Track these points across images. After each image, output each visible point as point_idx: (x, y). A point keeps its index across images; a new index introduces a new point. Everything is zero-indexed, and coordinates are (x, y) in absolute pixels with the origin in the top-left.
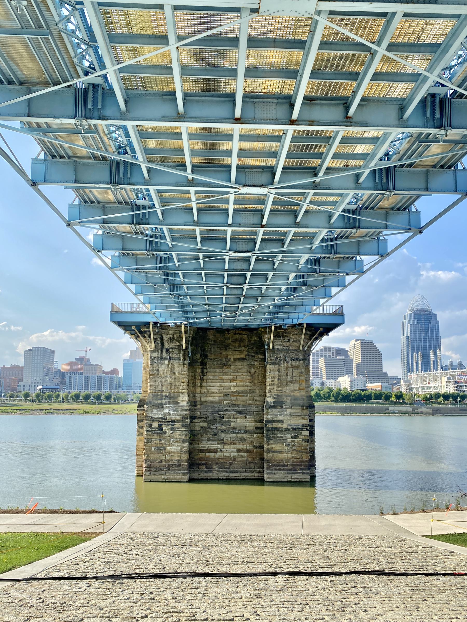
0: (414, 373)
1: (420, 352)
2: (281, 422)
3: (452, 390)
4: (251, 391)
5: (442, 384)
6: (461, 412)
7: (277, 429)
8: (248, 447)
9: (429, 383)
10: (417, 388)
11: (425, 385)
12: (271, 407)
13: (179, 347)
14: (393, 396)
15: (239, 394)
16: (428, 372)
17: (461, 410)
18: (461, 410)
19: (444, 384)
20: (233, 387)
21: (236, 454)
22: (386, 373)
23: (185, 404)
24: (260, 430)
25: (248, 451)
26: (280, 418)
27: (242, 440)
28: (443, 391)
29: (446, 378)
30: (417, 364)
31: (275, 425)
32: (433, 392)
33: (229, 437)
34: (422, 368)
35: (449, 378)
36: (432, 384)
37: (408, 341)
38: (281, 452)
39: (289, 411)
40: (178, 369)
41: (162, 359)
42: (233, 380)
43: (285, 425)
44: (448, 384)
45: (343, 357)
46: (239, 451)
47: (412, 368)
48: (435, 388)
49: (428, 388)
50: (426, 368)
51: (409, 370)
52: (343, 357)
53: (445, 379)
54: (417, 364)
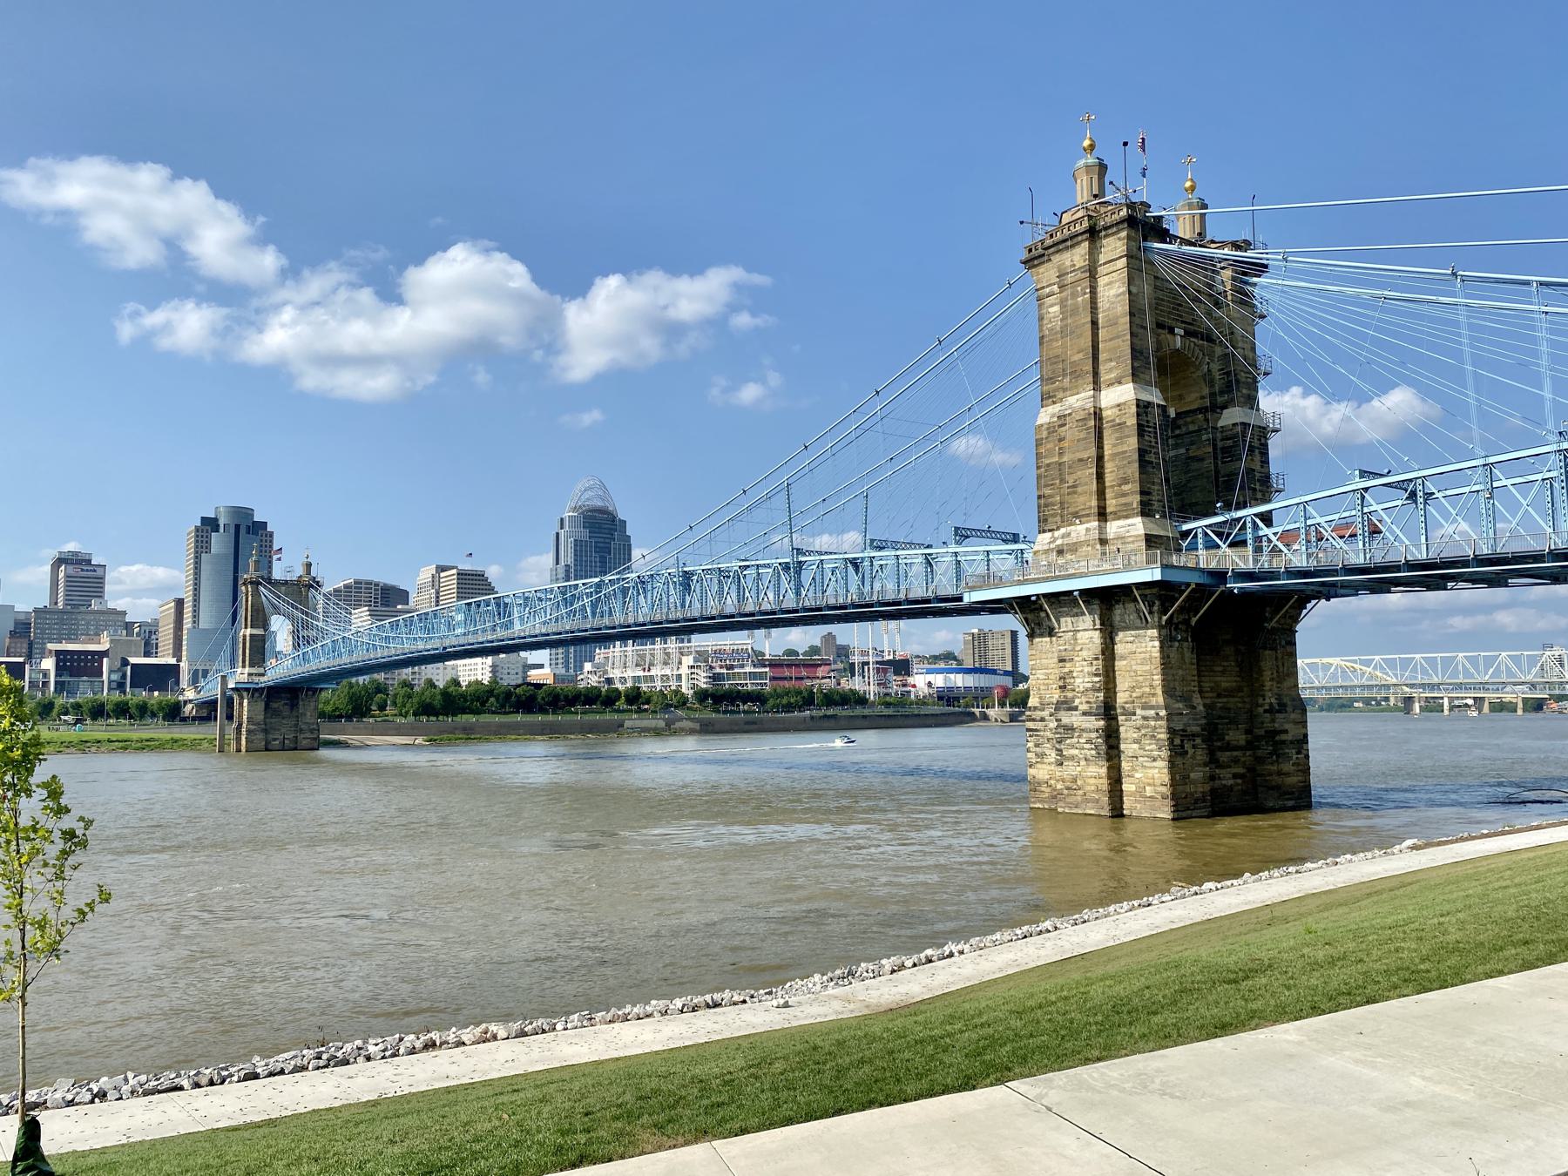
2: (1286, 732)
4: (1240, 689)
7: (1283, 742)
8: (1241, 770)
12: (1279, 712)
13: (1187, 622)
15: (1230, 693)
20: (1226, 682)
21: (1231, 782)
23: (1201, 708)
24: (1250, 745)
25: (1241, 776)
26: (1287, 726)
27: (1236, 761)
31: (1284, 737)
33: (1224, 757)
38: (1288, 774)
39: (1293, 716)
40: (1188, 655)
41: (1172, 639)
42: (1223, 673)
43: (1288, 737)
46: (1235, 776)
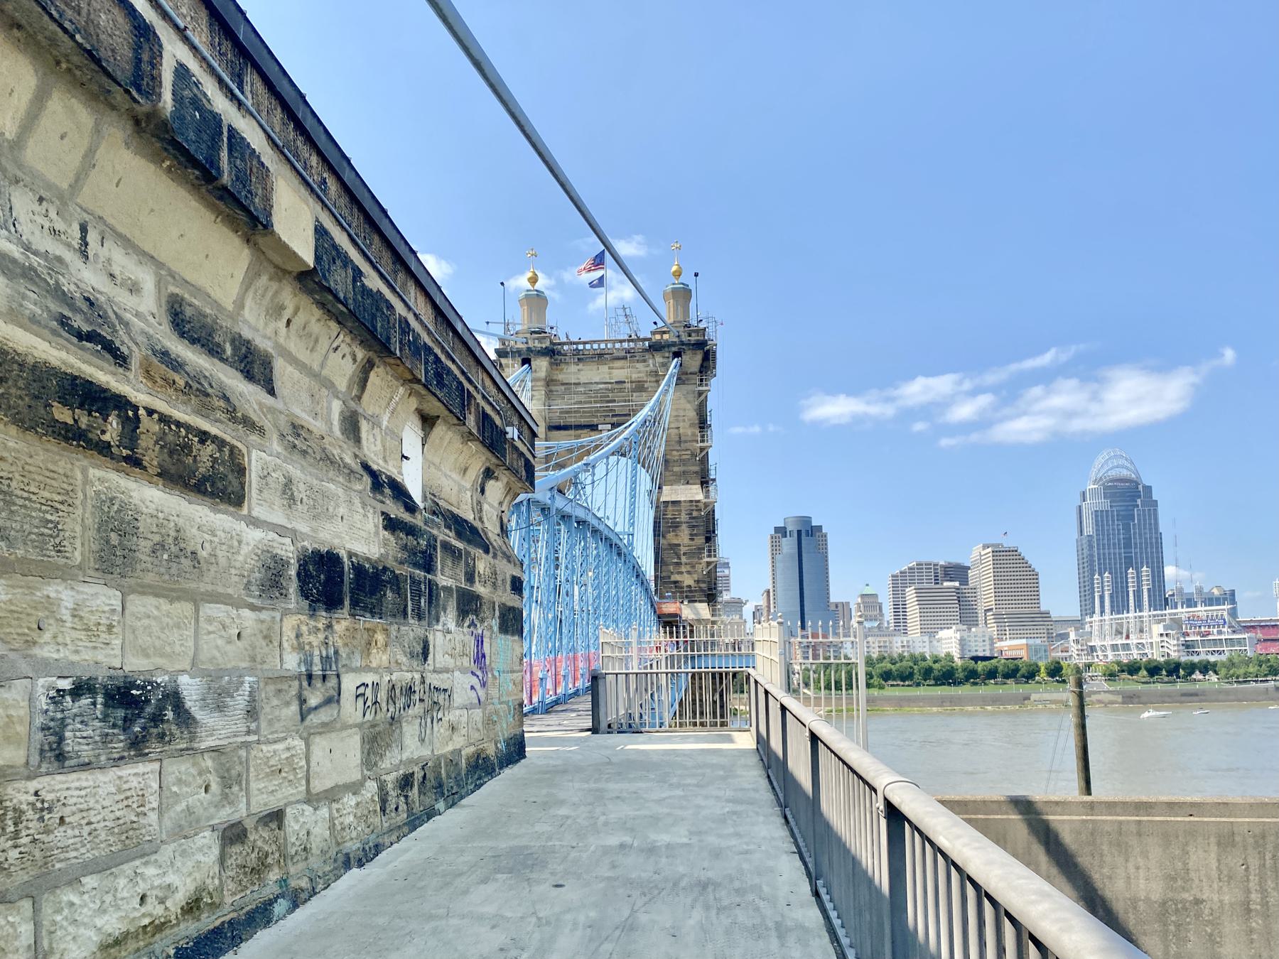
0: (1096, 617)
1: (1106, 574)
3: (1174, 651)
5: (1155, 639)
6: (1183, 698)
9: (1128, 637)
10: (1104, 649)
11: (1120, 641)
14: (1043, 669)
16: (1125, 615)
17: (1183, 695)
18: (1183, 695)
19: (1156, 639)
22: (1046, 615)
28: (1157, 656)
29: (1161, 625)
30: (1102, 597)
32: (1135, 654)
34: (1112, 607)
35: (1166, 628)
36: (1134, 640)
37: (1091, 547)
44: (1165, 638)
45: (957, 584)
47: (1102, 606)
48: (1140, 646)
49: (1126, 647)
50: (1119, 605)
51: (1088, 609)
52: (957, 584)
53: (1158, 629)
54: (1102, 597)
